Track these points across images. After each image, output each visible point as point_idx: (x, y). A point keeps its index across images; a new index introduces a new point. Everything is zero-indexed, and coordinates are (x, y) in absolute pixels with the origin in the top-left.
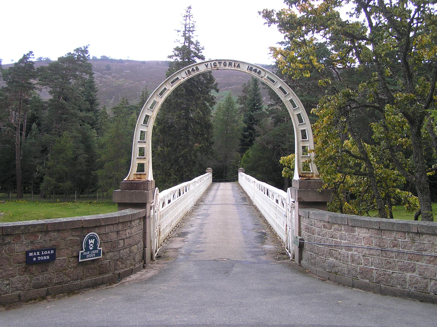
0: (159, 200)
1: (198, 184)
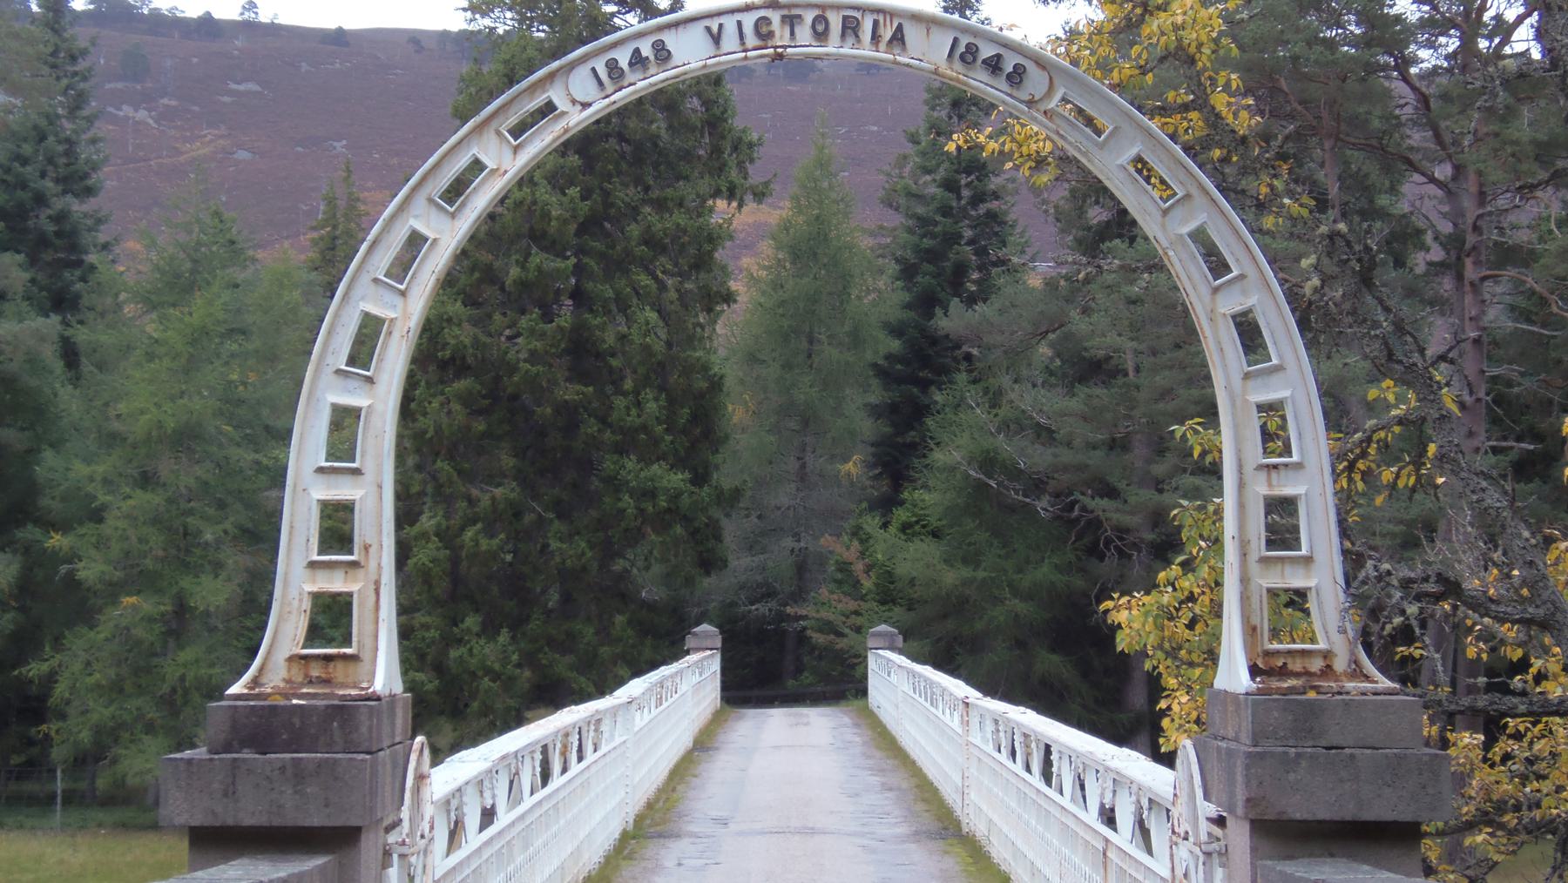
0: (428, 810)
1: (647, 717)
